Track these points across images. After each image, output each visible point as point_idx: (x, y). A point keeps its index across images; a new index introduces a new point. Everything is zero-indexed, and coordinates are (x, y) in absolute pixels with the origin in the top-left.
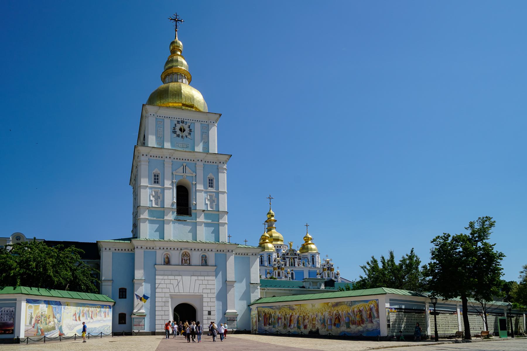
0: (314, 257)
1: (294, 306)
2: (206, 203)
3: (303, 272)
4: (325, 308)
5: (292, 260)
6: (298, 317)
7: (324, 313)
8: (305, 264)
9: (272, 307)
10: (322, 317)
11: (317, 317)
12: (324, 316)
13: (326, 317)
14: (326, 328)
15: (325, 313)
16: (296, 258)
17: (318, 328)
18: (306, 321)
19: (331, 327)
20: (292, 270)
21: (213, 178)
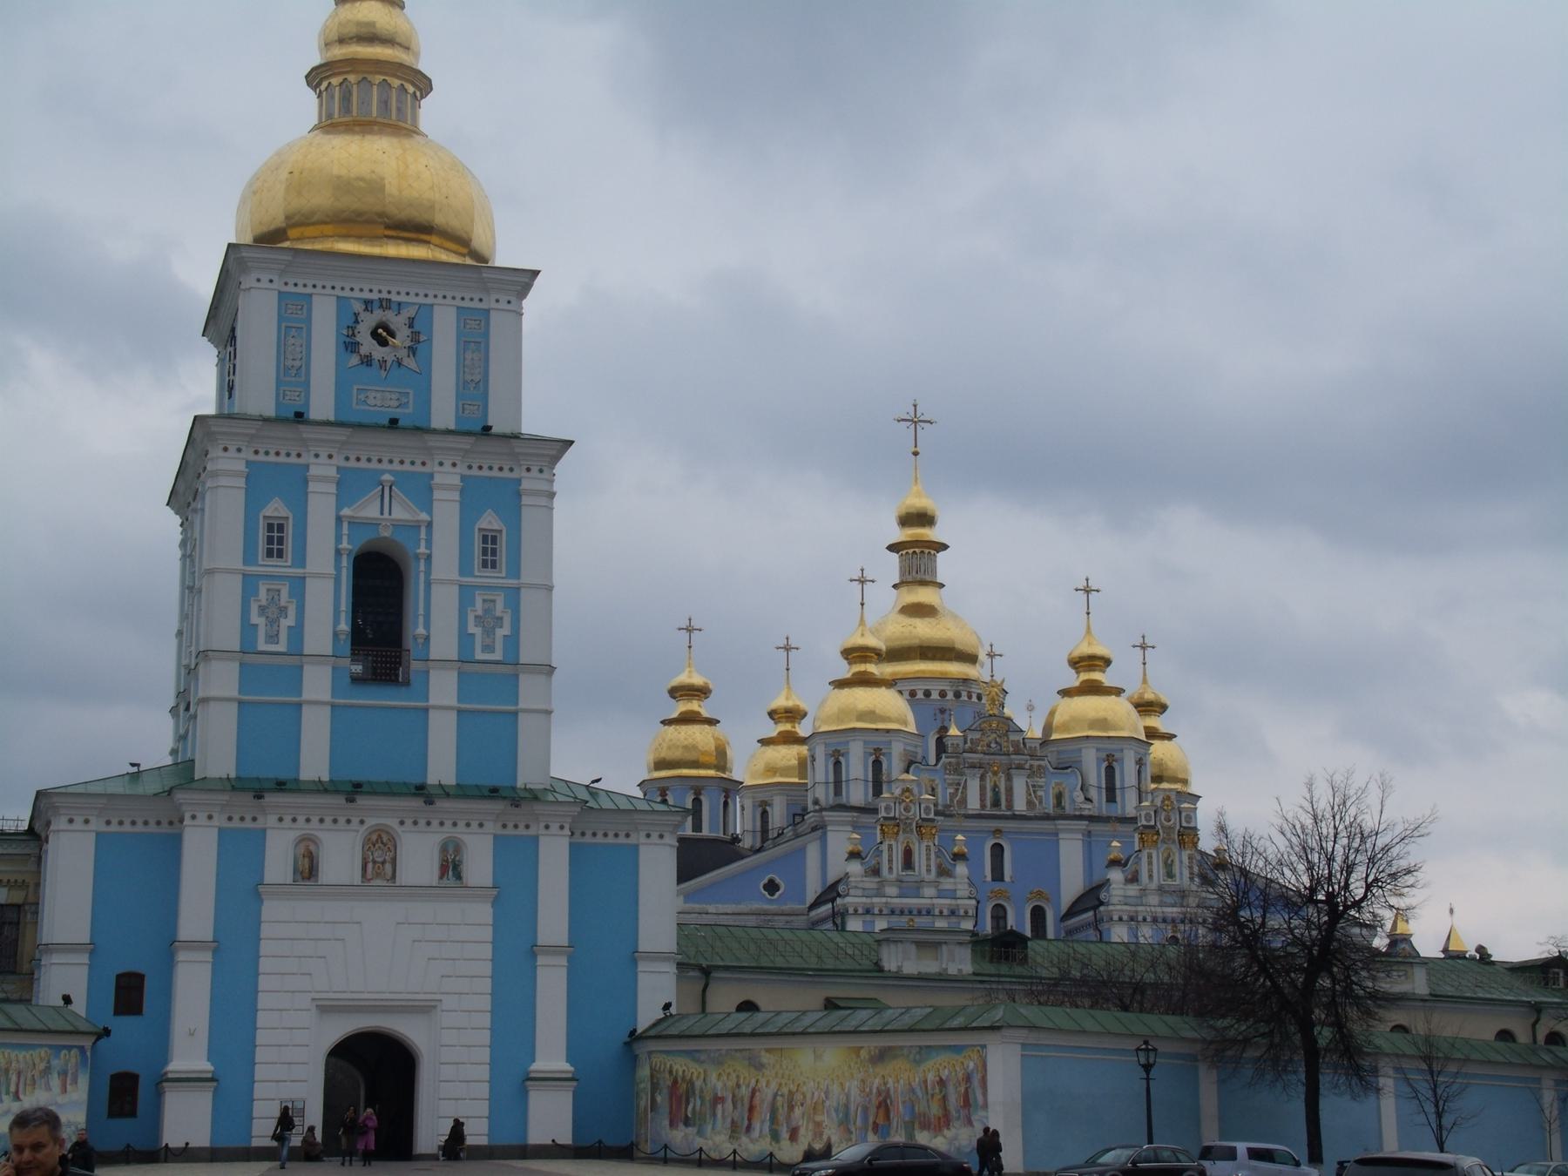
0: (1115, 764)
1: (763, 1053)
2: (470, 631)
3: (1058, 840)
4: (850, 1066)
5: (995, 773)
6: (775, 1095)
7: (847, 1084)
8: (1066, 802)
10: (841, 1097)
11: (826, 1097)
12: (848, 1096)
13: (852, 1099)
16: (1020, 767)
17: (829, 1139)
18: (798, 1111)
20: (998, 832)
21: (500, 531)
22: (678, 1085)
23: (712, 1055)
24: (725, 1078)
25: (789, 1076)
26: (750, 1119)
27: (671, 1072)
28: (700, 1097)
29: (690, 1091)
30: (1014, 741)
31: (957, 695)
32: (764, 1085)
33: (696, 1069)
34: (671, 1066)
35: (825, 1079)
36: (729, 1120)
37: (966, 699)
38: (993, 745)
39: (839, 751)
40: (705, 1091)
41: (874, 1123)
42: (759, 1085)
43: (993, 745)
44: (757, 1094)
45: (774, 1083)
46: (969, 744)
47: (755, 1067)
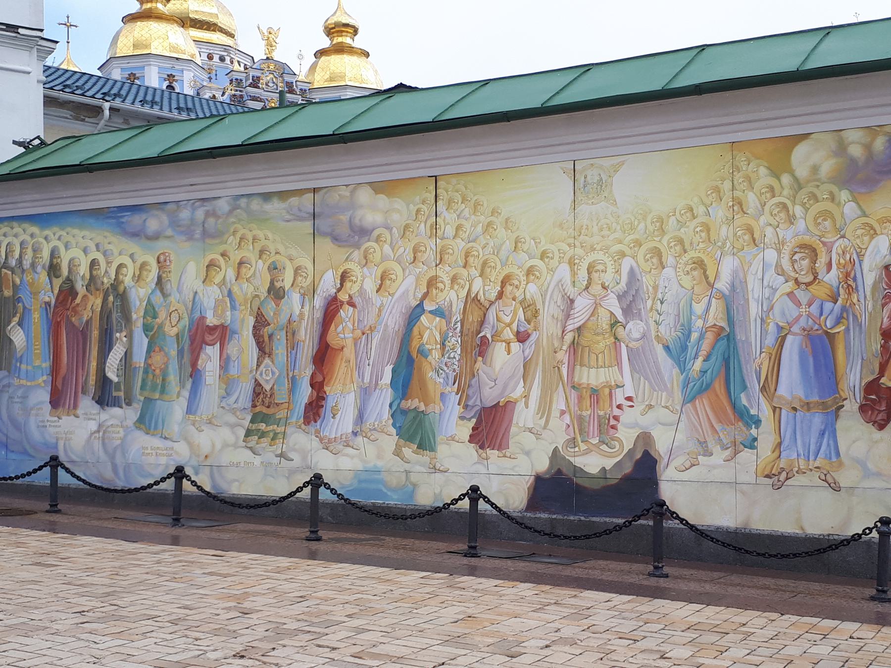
1: (364, 196)
4: (739, 204)
6: (414, 315)
7: (728, 266)
9: (127, 217)
10: (699, 308)
11: (628, 311)
13: (754, 310)
14: (752, 444)
15: (735, 274)
17: (645, 438)
19: (829, 430)
22: (78, 300)
23: (185, 214)
24: (231, 274)
25: (467, 257)
26: (318, 386)
27: (53, 269)
28: (147, 328)
29: (114, 316)
30: (289, 83)
31: (222, 59)
32: (370, 286)
33: (132, 256)
34: (54, 254)
35: (623, 255)
36: (245, 390)
37: (229, 63)
38: (271, 84)
39: (135, 74)
40: (162, 315)
41: (872, 387)
42: (352, 288)
43: (271, 84)
44: (346, 313)
45: (411, 280)
46: (251, 81)
47: (336, 239)
